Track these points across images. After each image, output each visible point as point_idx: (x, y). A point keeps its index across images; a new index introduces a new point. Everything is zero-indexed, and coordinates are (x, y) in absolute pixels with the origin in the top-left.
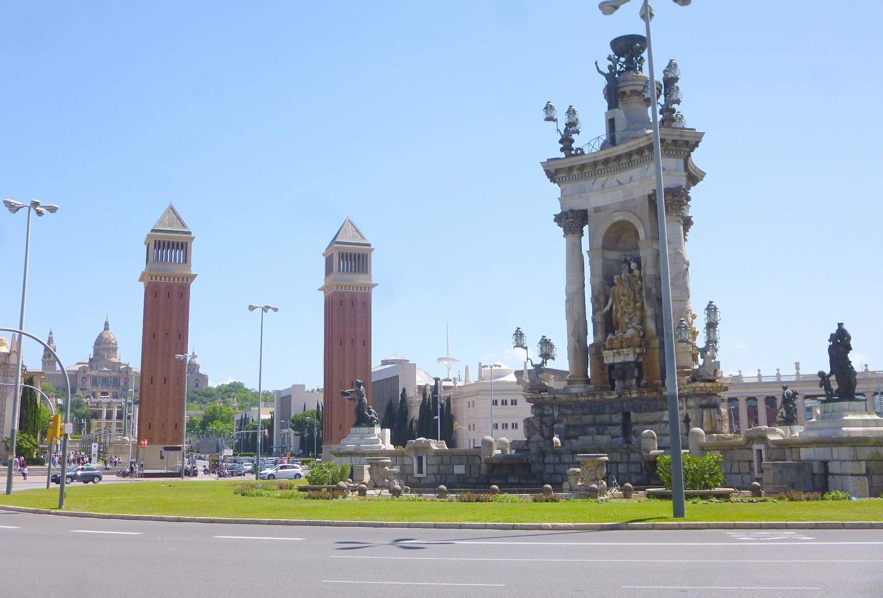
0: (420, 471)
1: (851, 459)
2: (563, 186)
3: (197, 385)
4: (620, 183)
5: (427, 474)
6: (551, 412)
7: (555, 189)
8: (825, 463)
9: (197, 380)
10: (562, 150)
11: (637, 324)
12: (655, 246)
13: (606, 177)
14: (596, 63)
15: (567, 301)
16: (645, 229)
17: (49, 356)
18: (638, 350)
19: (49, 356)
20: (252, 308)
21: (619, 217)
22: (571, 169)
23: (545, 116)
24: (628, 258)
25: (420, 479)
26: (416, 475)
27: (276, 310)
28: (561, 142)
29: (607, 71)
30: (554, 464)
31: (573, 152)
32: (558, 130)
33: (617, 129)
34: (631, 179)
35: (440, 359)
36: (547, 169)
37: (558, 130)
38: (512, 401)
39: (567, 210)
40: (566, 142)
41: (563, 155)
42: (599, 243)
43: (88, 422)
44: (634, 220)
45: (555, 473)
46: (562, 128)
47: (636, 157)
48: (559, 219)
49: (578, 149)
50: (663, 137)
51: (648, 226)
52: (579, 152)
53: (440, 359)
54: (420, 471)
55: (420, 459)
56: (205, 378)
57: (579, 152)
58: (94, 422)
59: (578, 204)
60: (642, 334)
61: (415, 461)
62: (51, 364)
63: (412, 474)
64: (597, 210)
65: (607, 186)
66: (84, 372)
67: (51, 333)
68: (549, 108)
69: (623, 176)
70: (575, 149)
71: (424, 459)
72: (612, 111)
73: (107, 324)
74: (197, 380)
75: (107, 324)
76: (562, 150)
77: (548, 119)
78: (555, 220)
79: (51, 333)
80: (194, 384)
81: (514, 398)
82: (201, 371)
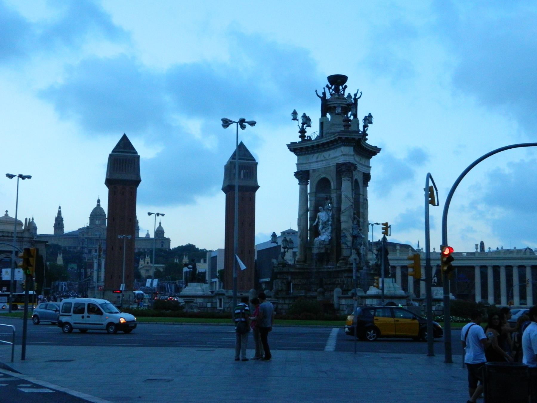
0: (220, 306)
1: (378, 304)
2: (299, 157)
3: (162, 246)
5: (224, 308)
6: (287, 277)
7: (293, 158)
9: (162, 242)
10: (300, 137)
11: (328, 233)
12: (338, 192)
14: (316, 91)
15: (298, 219)
16: (334, 183)
17: (59, 222)
19: (59, 222)
20: (150, 214)
21: (324, 176)
22: (302, 148)
23: (292, 118)
24: (328, 197)
25: (220, 310)
27: (163, 215)
28: (300, 132)
29: (321, 95)
30: (282, 304)
31: (306, 138)
32: (298, 126)
33: (324, 129)
34: (329, 156)
36: (290, 148)
37: (298, 126)
39: (299, 170)
40: (302, 132)
41: (300, 140)
42: (314, 190)
44: (329, 178)
45: (282, 309)
46: (301, 125)
47: (331, 145)
48: (297, 175)
49: (308, 137)
50: (340, 136)
51: (335, 182)
52: (309, 138)
54: (220, 306)
55: (220, 300)
56: (168, 240)
57: (309, 138)
59: (305, 168)
60: (330, 238)
61: (218, 301)
62: (60, 230)
63: (216, 308)
64: (314, 171)
66: (83, 235)
67: (60, 208)
68: (295, 113)
69: (326, 154)
70: (307, 136)
71: (223, 300)
72: (322, 118)
74: (162, 242)
76: (300, 137)
77: (293, 119)
78: (295, 175)
79: (60, 208)
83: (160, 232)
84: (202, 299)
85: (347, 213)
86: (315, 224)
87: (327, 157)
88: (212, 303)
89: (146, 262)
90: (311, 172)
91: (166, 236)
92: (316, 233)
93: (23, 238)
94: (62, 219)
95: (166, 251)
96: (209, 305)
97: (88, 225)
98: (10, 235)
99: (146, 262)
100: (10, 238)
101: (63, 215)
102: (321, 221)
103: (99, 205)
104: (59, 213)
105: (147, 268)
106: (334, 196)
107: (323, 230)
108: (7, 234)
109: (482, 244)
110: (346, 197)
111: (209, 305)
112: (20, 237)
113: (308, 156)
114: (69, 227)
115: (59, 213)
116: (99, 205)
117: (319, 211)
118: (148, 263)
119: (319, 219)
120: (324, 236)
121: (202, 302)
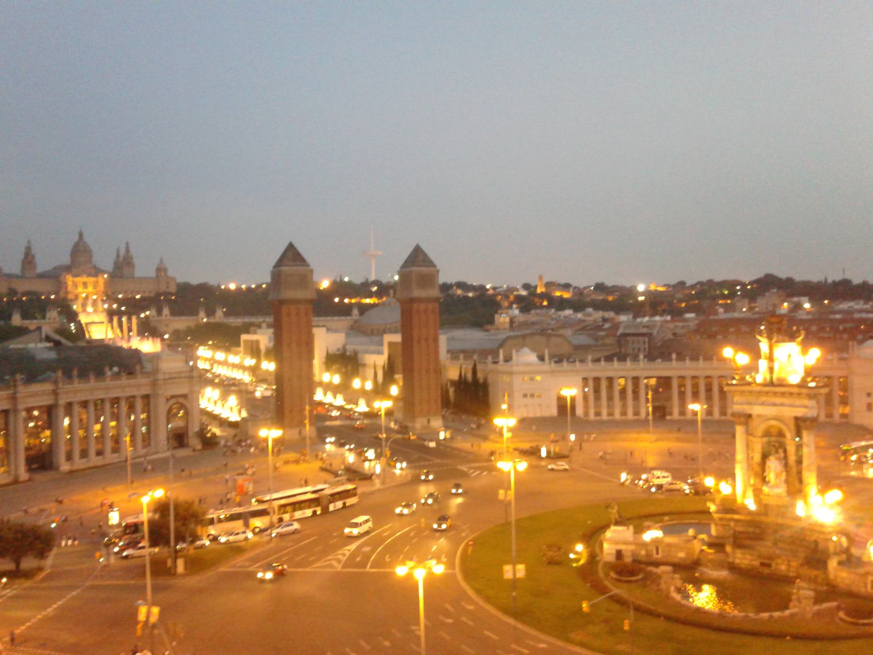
0: (657, 553)
17: (28, 259)
19: (28, 259)
25: (657, 558)
26: (655, 556)
54: (657, 553)
56: (173, 279)
64: (759, 416)
83: (161, 270)
88: (647, 551)
90: (754, 416)
91: (170, 273)
94: (33, 257)
96: (643, 552)
101: (33, 252)
106: (791, 449)
118: (166, 316)
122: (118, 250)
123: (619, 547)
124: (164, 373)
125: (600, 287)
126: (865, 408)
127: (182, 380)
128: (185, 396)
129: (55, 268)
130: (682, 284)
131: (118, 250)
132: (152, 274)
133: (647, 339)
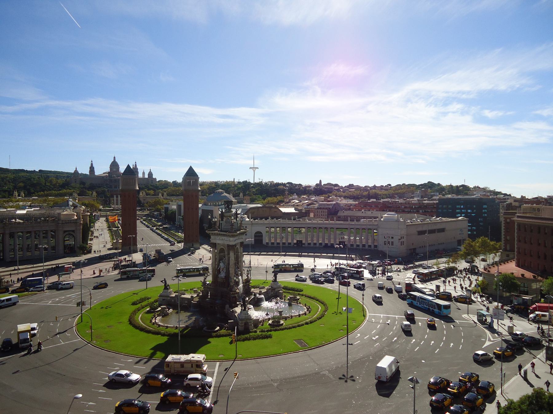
0: (178, 301)
4: (223, 240)
8: (239, 322)
13: (220, 237)
17: (92, 169)
18: (224, 279)
19: (92, 169)
35: (250, 168)
38: (245, 226)
43: (109, 199)
53: (250, 168)
56: (155, 179)
58: (112, 199)
61: (177, 299)
64: (218, 244)
65: (220, 239)
67: (92, 161)
73: (114, 158)
74: (152, 180)
75: (114, 158)
79: (92, 161)
80: (151, 182)
81: (246, 226)
82: (154, 177)
83: (150, 174)
84: (170, 298)
85: (232, 267)
86: (219, 268)
87: (224, 239)
89: (143, 195)
91: (154, 177)
92: (219, 272)
93: (77, 223)
94: (94, 168)
95: (154, 186)
96: (173, 301)
97: (109, 171)
98: (69, 222)
99: (143, 195)
100: (70, 224)
102: (221, 268)
103: (115, 160)
104: (92, 164)
105: (144, 198)
106: (226, 257)
107: (222, 272)
108: (67, 222)
109: (320, 181)
110: (232, 260)
111: (173, 301)
112: (75, 223)
113: (216, 236)
114: (99, 172)
115: (92, 164)
116: (115, 160)
117: (220, 263)
118: (144, 195)
119: (220, 266)
120: (222, 275)
121: (169, 299)
122: (133, 165)
123: (164, 298)
124: (62, 221)
125: (351, 186)
126: (384, 243)
127: (72, 224)
128: (73, 231)
129: (104, 173)
130: (390, 185)
131: (133, 165)
132: (146, 176)
133: (327, 210)
